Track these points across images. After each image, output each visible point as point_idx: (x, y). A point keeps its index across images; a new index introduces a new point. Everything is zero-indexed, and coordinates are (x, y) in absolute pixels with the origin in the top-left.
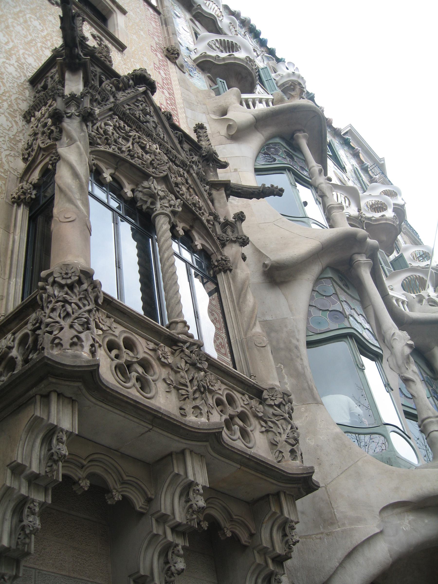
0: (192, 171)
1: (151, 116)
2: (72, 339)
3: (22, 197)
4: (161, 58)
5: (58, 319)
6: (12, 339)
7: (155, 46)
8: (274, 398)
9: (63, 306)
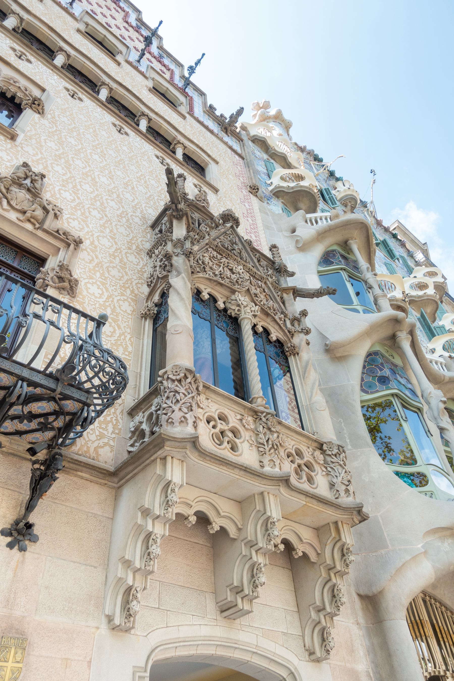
0: (268, 282)
1: (236, 244)
2: (180, 419)
3: (148, 313)
4: (245, 193)
5: (171, 405)
6: (142, 417)
7: (240, 185)
8: (331, 450)
9: (174, 395)
